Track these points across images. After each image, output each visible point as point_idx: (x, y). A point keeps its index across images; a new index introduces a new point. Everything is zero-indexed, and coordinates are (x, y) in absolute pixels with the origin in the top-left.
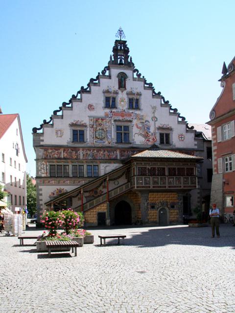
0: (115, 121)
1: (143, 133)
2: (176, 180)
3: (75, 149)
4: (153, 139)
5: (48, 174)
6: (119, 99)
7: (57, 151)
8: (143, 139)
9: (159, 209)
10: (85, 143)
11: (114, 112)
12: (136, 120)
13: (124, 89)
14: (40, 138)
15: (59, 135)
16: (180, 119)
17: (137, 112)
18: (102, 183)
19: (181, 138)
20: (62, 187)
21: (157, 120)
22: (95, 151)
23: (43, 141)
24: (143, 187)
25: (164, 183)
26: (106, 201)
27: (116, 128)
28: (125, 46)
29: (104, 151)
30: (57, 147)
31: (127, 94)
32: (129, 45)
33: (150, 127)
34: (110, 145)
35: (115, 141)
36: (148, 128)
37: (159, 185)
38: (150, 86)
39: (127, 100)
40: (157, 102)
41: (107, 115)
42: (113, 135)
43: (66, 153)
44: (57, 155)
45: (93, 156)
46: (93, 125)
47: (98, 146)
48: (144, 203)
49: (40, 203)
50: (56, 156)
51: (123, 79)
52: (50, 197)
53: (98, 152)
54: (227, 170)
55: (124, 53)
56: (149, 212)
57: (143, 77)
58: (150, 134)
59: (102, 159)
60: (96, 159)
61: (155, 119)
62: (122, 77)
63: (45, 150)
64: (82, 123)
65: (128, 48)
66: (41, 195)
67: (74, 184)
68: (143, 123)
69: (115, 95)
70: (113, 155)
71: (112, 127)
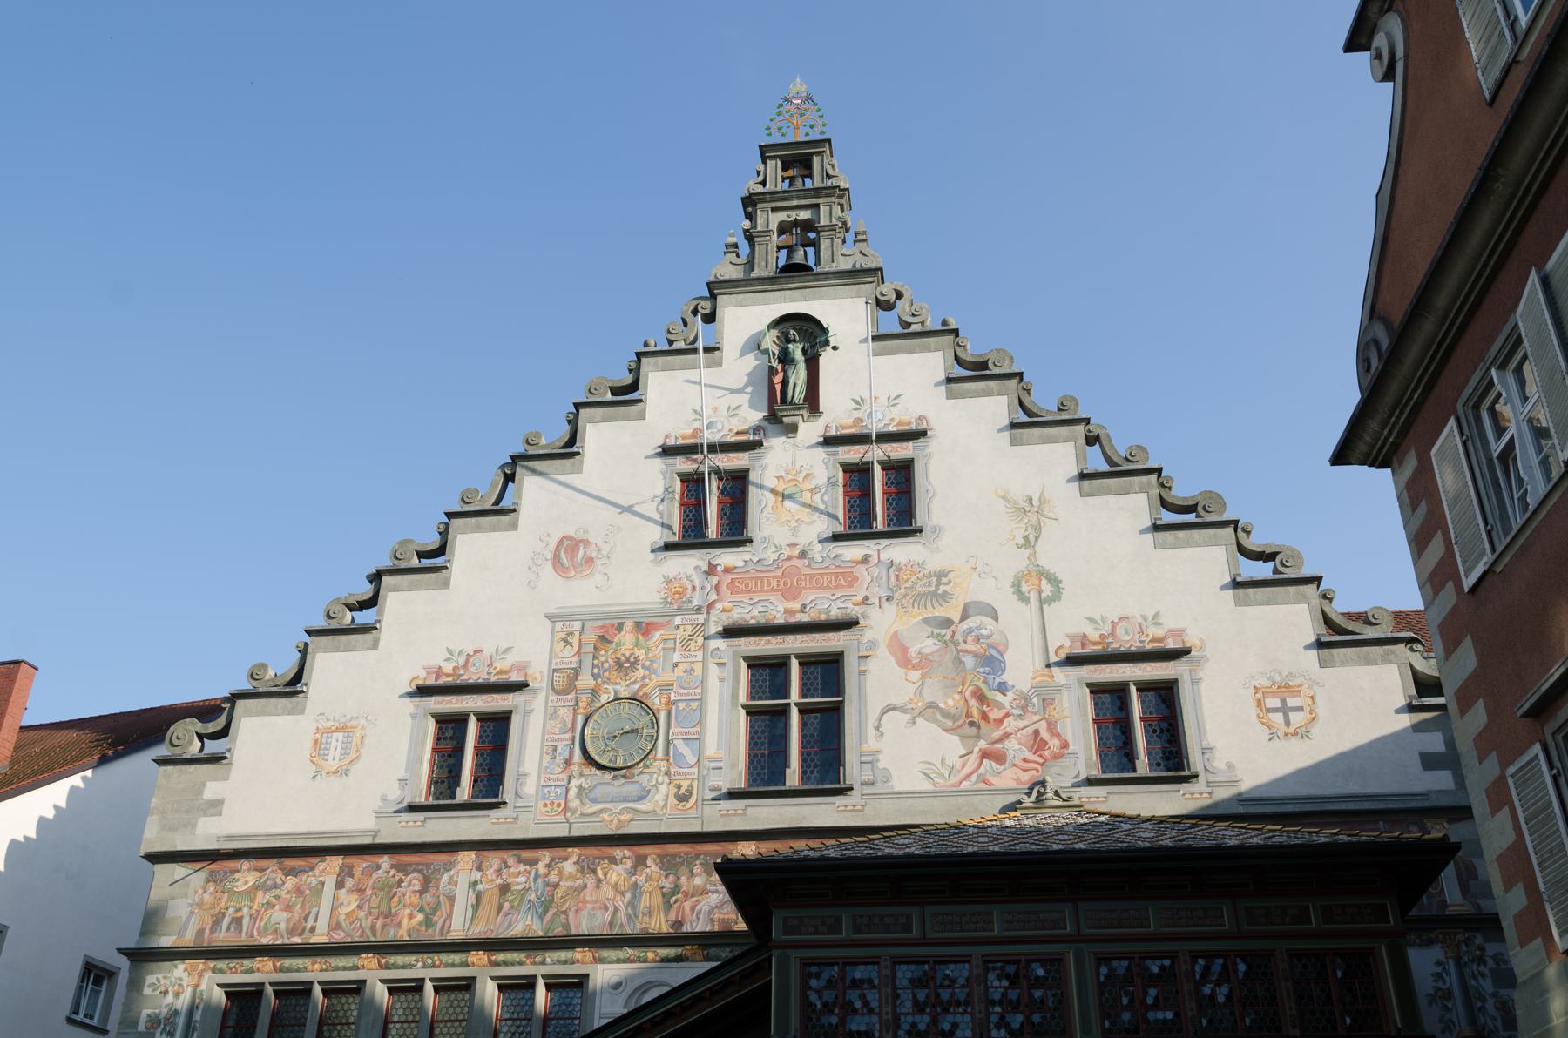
1: (951, 702)
4: (1038, 744)
7: (291, 882)
8: (952, 746)
11: (727, 570)
12: (891, 609)
15: (332, 763)
17: (900, 551)
19: (1285, 710)
21: (1057, 596)
22: (569, 867)
36: (992, 661)
41: (677, 596)
43: (360, 890)
44: (288, 908)
45: (547, 905)
46: (577, 672)
50: (279, 916)
51: (797, 350)
53: (587, 868)
58: (1006, 700)
63: (211, 878)
68: (947, 623)
70: (704, 892)
71: (714, 671)
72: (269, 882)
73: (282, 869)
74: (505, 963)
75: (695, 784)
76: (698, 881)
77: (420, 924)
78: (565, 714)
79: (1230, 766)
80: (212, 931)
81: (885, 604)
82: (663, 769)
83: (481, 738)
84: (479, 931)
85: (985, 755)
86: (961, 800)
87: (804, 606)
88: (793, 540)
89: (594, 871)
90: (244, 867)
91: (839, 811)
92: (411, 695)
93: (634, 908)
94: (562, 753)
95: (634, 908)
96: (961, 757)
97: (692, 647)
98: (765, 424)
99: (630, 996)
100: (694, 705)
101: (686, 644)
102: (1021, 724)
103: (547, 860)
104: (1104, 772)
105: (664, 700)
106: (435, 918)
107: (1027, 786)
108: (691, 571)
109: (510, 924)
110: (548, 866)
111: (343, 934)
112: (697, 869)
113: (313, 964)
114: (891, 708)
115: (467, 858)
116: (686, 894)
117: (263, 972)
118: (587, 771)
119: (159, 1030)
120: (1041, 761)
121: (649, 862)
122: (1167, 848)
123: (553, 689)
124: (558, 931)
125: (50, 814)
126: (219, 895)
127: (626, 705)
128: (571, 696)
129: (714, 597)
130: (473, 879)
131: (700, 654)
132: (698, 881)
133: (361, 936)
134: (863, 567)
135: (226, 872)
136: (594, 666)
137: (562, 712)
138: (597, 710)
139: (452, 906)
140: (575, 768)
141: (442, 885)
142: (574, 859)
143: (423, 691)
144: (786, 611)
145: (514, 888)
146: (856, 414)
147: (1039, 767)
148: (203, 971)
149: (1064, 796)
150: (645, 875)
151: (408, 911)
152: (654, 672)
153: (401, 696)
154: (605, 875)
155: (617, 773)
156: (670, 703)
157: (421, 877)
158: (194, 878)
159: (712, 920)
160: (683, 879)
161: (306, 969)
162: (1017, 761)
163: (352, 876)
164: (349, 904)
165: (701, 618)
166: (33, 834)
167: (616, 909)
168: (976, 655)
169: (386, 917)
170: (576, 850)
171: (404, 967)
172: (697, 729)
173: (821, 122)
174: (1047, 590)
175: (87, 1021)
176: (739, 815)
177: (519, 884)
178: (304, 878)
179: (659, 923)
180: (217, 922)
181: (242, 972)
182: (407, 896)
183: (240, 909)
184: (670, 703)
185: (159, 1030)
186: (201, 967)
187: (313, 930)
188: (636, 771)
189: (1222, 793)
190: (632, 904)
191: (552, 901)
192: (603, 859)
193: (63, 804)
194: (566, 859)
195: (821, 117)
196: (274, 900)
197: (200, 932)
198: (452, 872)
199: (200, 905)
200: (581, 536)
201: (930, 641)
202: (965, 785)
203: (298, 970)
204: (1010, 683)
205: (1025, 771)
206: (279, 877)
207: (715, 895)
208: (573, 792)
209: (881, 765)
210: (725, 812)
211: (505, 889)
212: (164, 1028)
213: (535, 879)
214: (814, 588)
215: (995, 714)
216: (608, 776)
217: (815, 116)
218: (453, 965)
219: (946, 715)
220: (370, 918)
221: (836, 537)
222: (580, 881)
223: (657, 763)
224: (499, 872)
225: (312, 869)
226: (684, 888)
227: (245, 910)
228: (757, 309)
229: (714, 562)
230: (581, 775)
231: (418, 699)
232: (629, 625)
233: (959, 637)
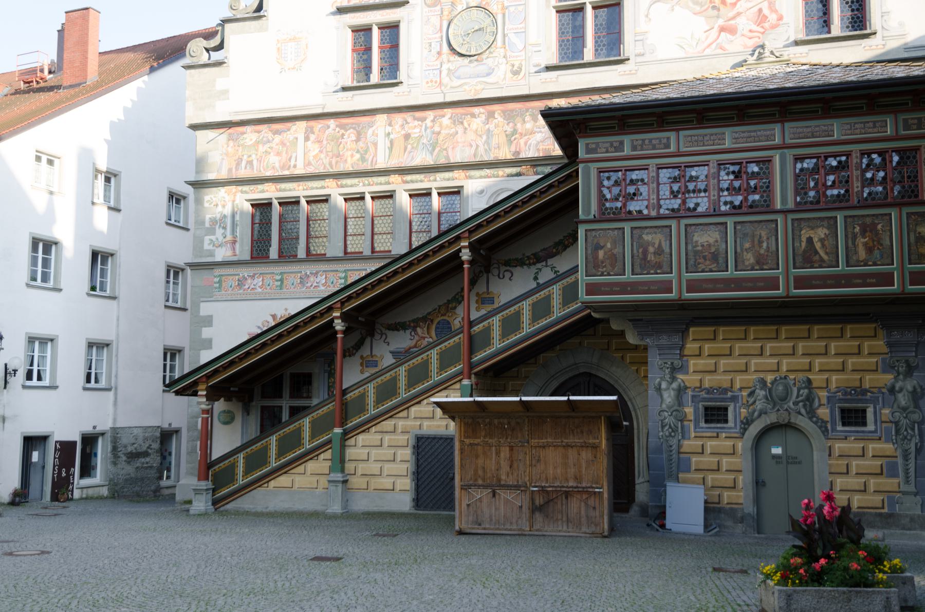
2: (851, 238)
4: (761, 18)
5: (237, 246)
7: (278, 138)
8: (701, 24)
9: (754, 430)
22: (446, 121)
24: (624, 288)
25: (760, 263)
26: (460, 373)
37: (731, 273)
43: (320, 142)
44: (278, 154)
48: (659, 389)
56: (689, 444)
66: (208, 344)
70: (532, 133)
72: (265, 139)
73: (271, 131)
74: (412, 181)
75: (523, 63)
76: (529, 126)
77: (358, 160)
78: (435, 21)
79: (901, 24)
80: (237, 169)
82: (502, 54)
83: (382, 40)
84: (394, 163)
85: (722, 29)
89: (462, 123)
90: (248, 131)
91: (620, 75)
92: (333, 14)
93: (488, 144)
95: (488, 144)
96: (705, 32)
99: (490, 198)
100: (520, 8)
103: (432, 118)
104: (807, 35)
105: (500, 7)
106: (367, 156)
107: (751, 49)
109: (413, 158)
110: (433, 121)
111: (313, 168)
112: (528, 118)
113: (299, 186)
115: (382, 118)
116: (521, 134)
117: (269, 192)
119: (217, 226)
120: (762, 30)
121: (496, 116)
122: (852, 82)
123: (425, 4)
124: (442, 161)
125: (129, 105)
126: (237, 148)
127: (474, 11)
128: (438, 8)
130: (387, 132)
132: (529, 126)
133: (324, 169)
135: (238, 134)
138: (456, 16)
139: (376, 149)
140: (444, 57)
141: (368, 136)
142: (449, 116)
143: (341, 11)
145: (412, 136)
147: (760, 35)
148: (236, 192)
149: (777, 54)
150: (493, 125)
151: (350, 153)
153: (327, 15)
154: (469, 125)
155: (472, 58)
156: (504, 8)
157: (355, 132)
158: (220, 137)
159: (538, 150)
160: (519, 126)
161: (294, 189)
162: (746, 32)
163: (313, 133)
166: (122, 118)
167: (477, 146)
169: (337, 157)
170: (450, 110)
171: (351, 186)
172: (523, 25)
175: (177, 224)
176: (554, 81)
177: (415, 133)
178: (285, 135)
179: (506, 154)
180: (238, 164)
181: (258, 192)
182: (349, 143)
183: (250, 156)
184: (504, 8)
185: (217, 226)
186: (234, 190)
187: (295, 166)
188: (484, 56)
189: (893, 44)
190: (487, 142)
191: (437, 143)
192: (467, 115)
193: (135, 99)
194: (444, 116)
196: (269, 150)
197: (230, 170)
198: (374, 128)
199: (227, 154)
202: (708, 52)
203: (290, 190)
205: (750, 38)
206: (270, 135)
207: (540, 134)
208: (444, 73)
210: (544, 80)
211: (407, 137)
212: (220, 225)
213: (426, 130)
216: (467, 60)
218: (381, 184)
220: (328, 158)
222: (454, 130)
223: (498, 50)
225: (289, 130)
226: (520, 131)
227: (254, 157)
230: (449, 61)
231: (338, 17)
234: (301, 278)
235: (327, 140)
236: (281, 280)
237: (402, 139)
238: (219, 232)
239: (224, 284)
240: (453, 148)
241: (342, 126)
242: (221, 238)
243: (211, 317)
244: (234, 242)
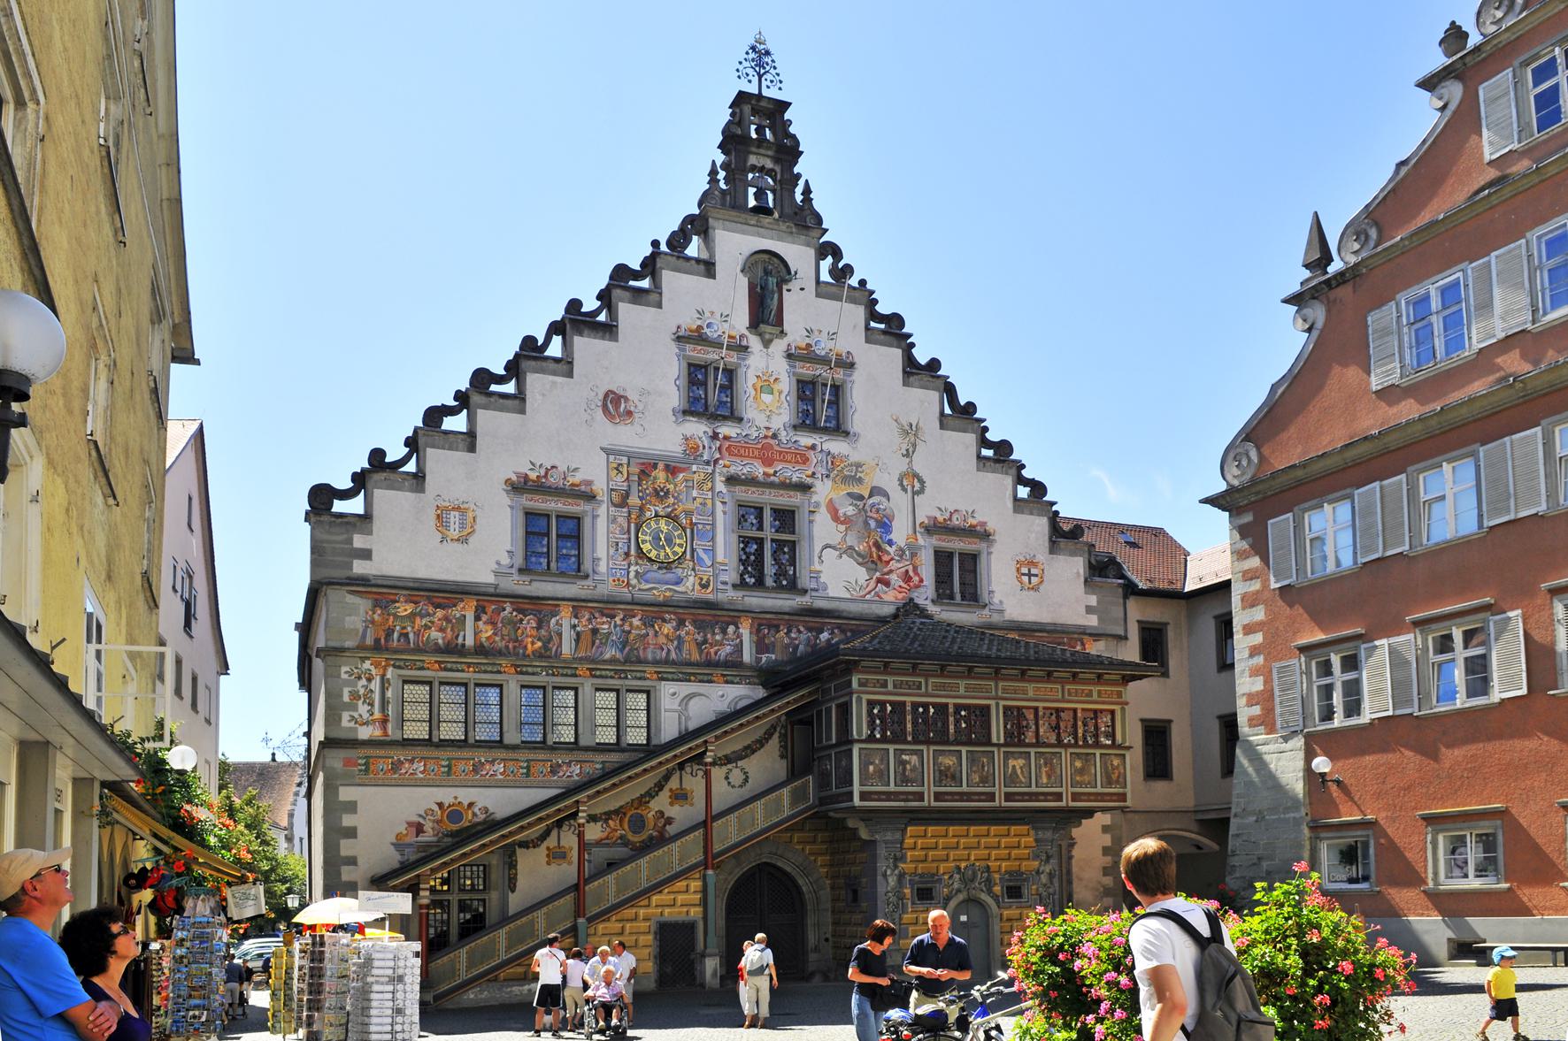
0: (731, 480)
1: (861, 548)
3: (540, 607)
5: (390, 726)
6: (752, 380)
8: (861, 574)
10: (587, 577)
11: (726, 438)
12: (829, 483)
13: (776, 330)
14: (350, 541)
16: (1023, 492)
17: (836, 446)
18: (667, 777)
20: (465, 795)
21: (922, 491)
22: (636, 621)
23: (366, 554)
25: (984, 780)
27: (733, 518)
28: (782, 127)
29: (681, 623)
30: (442, 594)
31: (789, 356)
32: (799, 122)
33: (891, 518)
34: (708, 595)
35: (731, 576)
36: (885, 525)
38: (892, 329)
39: (786, 385)
40: (927, 402)
41: (692, 450)
42: (725, 548)
45: (625, 643)
46: (627, 494)
47: (647, 597)
49: (345, 877)
52: (399, 845)
53: (648, 622)
54: (1328, 715)
55: (776, 160)
57: (863, 283)
58: (891, 550)
59: (667, 662)
60: (640, 661)
61: (913, 483)
62: (767, 273)
64: (577, 478)
65: (794, 137)
67: (527, 779)
68: (861, 498)
69: (733, 358)
70: (722, 644)
71: (719, 507)
76: (718, 637)
77: (540, 648)
78: (622, 521)
81: (825, 480)
85: (879, 581)
86: (866, 606)
87: (776, 472)
88: (767, 425)
89: (653, 626)
93: (680, 651)
94: (623, 548)
95: (680, 651)
97: (705, 488)
98: (747, 333)
100: (708, 527)
101: (700, 486)
102: (900, 565)
103: (622, 616)
108: (701, 434)
109: (601, 654)
112: (717, 631)
113: (469, 667)
114: (827, 546)
116: (711, 644)
118: (640, 562)
119: (360, 702)
121: (687, 624)
128: (624, 510)
129: (718, 456)
131: (710, 493)
132: (718, 637)
134: (812, 452)
136: (639, 491)
137: (620, 520)
139: (561, 639)
142: (639, 617)
144: (765, 474)
146: (808, 341)
151: (530, 640)
152: (679, 501)
156: (692, 524)
160: (709, 636)
161: (463, 671)
164: (486, 632)
165: (710, 469)
167: (669, 650)
168: (876, 520)
171: (533, 674)
172: (711, 543)
173: (778, 78)
174: (917, 486)
184: (692, 524)
190: (679, 648)
191: (627, 642)
195: (778, 75)
200: (622, 393)
201: (851, 508)
202: (868, 597)
203: (458, 671)
204: (895, 540)
208: (632, 574)
209: (822, 580)
211: (595, 631)
212: (364, 702)
213: (615, 627)
214: (781, 461)
215: (886, 558)
216: (655, 567)
217: (772, 71)
218: (566, 675)
219: (859, 554)
221: (795, 427)
224: (589, 620)
228: (737, 237)
229: (718, 431)
230: (637, 564)
232: (661, 466)
233: (867, 508)
234: (473, 765)
235: (502, 622)
236: (449, 766)
237: (589, 632)
238: (363, 709)
239: (372, 767)
240: (645, 649)
241: (520, 611)
242: (366, 716)
243: (355, 803)
244: (384, 721)
